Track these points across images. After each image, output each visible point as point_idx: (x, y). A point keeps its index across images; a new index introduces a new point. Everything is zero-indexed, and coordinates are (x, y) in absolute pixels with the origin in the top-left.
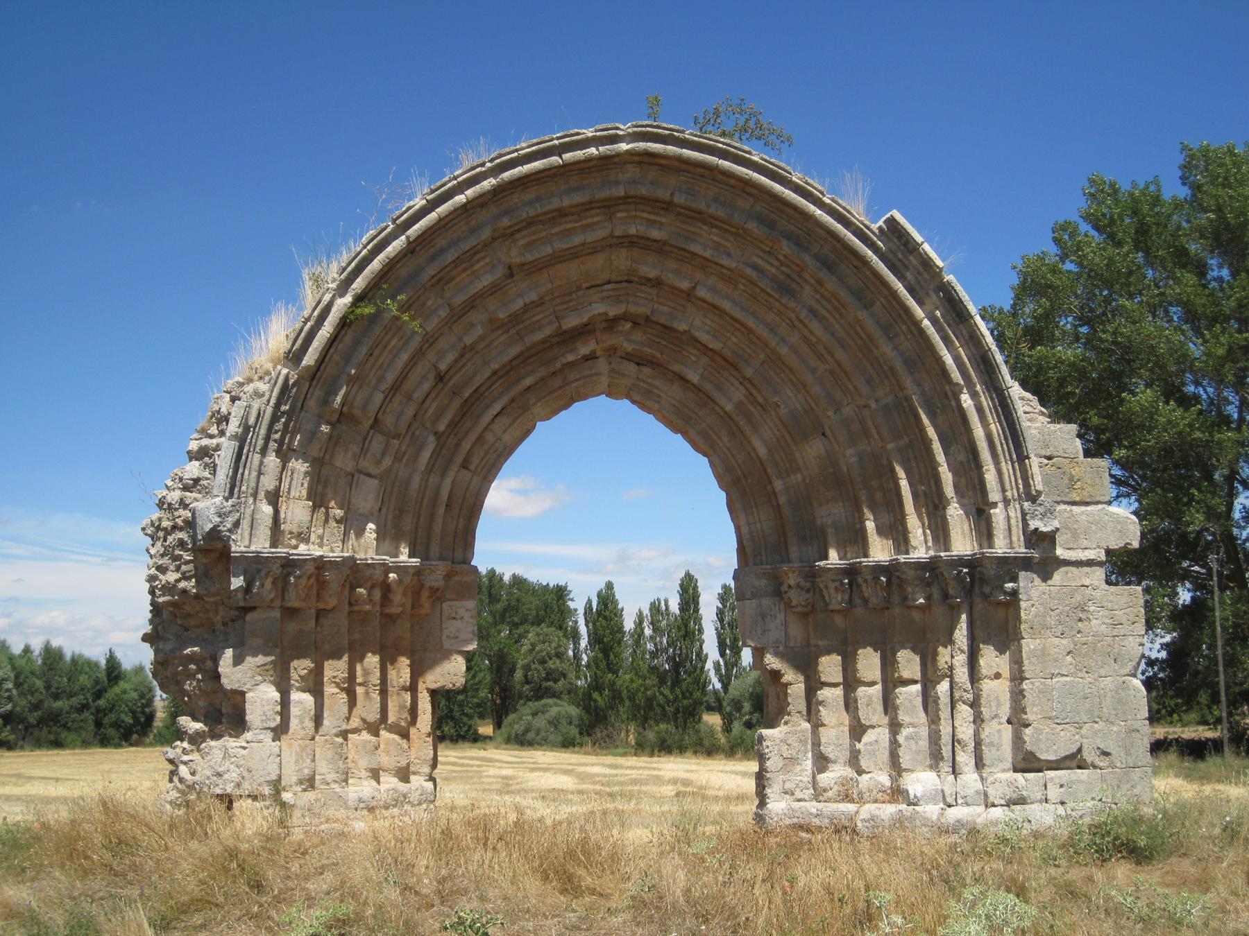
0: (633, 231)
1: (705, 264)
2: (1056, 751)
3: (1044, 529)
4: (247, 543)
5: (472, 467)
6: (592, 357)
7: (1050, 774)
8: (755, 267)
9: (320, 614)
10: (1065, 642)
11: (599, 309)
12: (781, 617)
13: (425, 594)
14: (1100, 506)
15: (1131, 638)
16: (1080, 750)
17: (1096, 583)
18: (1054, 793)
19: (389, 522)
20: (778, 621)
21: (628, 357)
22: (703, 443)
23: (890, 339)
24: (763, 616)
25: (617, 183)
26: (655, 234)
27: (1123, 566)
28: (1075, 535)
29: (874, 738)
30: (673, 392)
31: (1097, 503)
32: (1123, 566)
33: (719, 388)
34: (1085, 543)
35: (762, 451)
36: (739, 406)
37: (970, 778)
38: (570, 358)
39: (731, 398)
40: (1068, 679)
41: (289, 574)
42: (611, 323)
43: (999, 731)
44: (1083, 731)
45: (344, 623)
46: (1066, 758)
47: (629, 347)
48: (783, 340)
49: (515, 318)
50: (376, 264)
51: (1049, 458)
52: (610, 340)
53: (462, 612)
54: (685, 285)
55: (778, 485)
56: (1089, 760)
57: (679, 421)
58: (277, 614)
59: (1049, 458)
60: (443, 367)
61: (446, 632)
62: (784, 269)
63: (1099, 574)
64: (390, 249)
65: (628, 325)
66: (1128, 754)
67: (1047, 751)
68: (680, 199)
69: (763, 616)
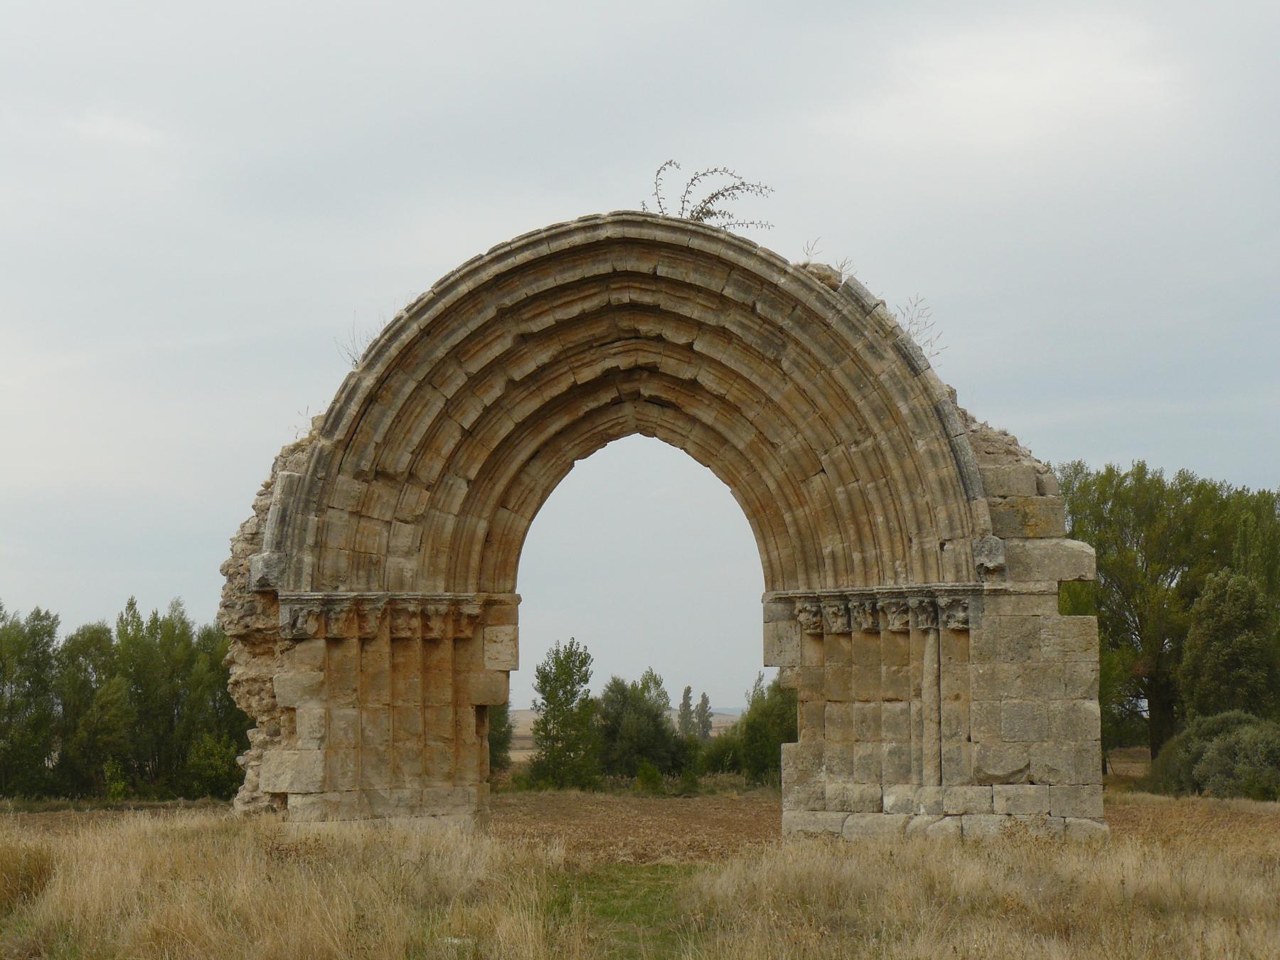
0: (626, 299)
1: (700, 325)
2: (1003, 767)
3: (990, 565)
4: (292, 587)
5: (510, 506)
6: (617, 402)
7: (997, 787)
8: (742, 326)
9: (364, 641)
10: (1015, 667)
11: (610, 363)
12: (797, 638)
13: (464, 621)
14: (1054, 541)
15: (1083, 665)
16: (1028, 766)
17: (1048, 613)
18: (999, 805)
19: (427, 561)
20: (795, 643)
21: (654, 401)
22: (729, 477)
23: (859, 389)
24: (780, 638)
25: (606, 261)
26: (647, 299)
27: (1075, 598)
28: (1028, 569)
29: (869, 752)
30: (696, 434)
31: (1051, 537)
32: (1075, 598)
33: (731, 429)
34: (1038, 576)
35: (772, 486)
36: (750, 446)
37: (930, 790)
38: (593, 405)
39: (742, 438)
40: (1016, 701)
41: (329, 611)
42: (631, 373)
43: (959, 748)
44: (1032, 750)
45: (386, 649)
46: (1014, 774)
47: (646, 392)
48: (776, 388)
49: (532, 377)
50: (394, 350)
51: (1005, 497)
52: (627, 388)
53: (502, 636)
54: (682, 340)
55: (788, 517)
56: (1036, 778)
57: (705, 457)
58: (321, 643)
59: (1005, 497)
60: (466, 426)
61: (487, 654)
62: (766, 326)
63: (1053, 603)
64: (404, 337)
65: (645, 374)
66: (1078, 773)
67: (994, 767)
68: (662, 271)
69: (780, 638)
